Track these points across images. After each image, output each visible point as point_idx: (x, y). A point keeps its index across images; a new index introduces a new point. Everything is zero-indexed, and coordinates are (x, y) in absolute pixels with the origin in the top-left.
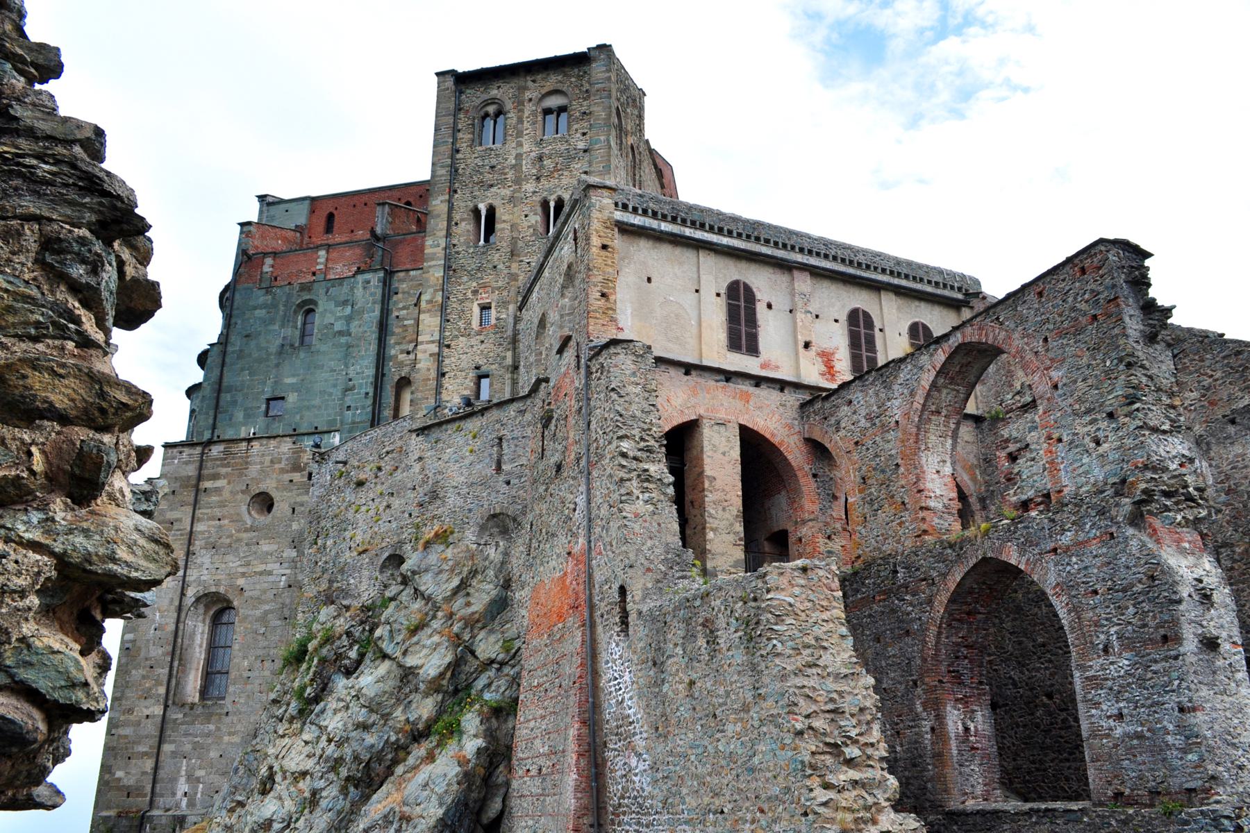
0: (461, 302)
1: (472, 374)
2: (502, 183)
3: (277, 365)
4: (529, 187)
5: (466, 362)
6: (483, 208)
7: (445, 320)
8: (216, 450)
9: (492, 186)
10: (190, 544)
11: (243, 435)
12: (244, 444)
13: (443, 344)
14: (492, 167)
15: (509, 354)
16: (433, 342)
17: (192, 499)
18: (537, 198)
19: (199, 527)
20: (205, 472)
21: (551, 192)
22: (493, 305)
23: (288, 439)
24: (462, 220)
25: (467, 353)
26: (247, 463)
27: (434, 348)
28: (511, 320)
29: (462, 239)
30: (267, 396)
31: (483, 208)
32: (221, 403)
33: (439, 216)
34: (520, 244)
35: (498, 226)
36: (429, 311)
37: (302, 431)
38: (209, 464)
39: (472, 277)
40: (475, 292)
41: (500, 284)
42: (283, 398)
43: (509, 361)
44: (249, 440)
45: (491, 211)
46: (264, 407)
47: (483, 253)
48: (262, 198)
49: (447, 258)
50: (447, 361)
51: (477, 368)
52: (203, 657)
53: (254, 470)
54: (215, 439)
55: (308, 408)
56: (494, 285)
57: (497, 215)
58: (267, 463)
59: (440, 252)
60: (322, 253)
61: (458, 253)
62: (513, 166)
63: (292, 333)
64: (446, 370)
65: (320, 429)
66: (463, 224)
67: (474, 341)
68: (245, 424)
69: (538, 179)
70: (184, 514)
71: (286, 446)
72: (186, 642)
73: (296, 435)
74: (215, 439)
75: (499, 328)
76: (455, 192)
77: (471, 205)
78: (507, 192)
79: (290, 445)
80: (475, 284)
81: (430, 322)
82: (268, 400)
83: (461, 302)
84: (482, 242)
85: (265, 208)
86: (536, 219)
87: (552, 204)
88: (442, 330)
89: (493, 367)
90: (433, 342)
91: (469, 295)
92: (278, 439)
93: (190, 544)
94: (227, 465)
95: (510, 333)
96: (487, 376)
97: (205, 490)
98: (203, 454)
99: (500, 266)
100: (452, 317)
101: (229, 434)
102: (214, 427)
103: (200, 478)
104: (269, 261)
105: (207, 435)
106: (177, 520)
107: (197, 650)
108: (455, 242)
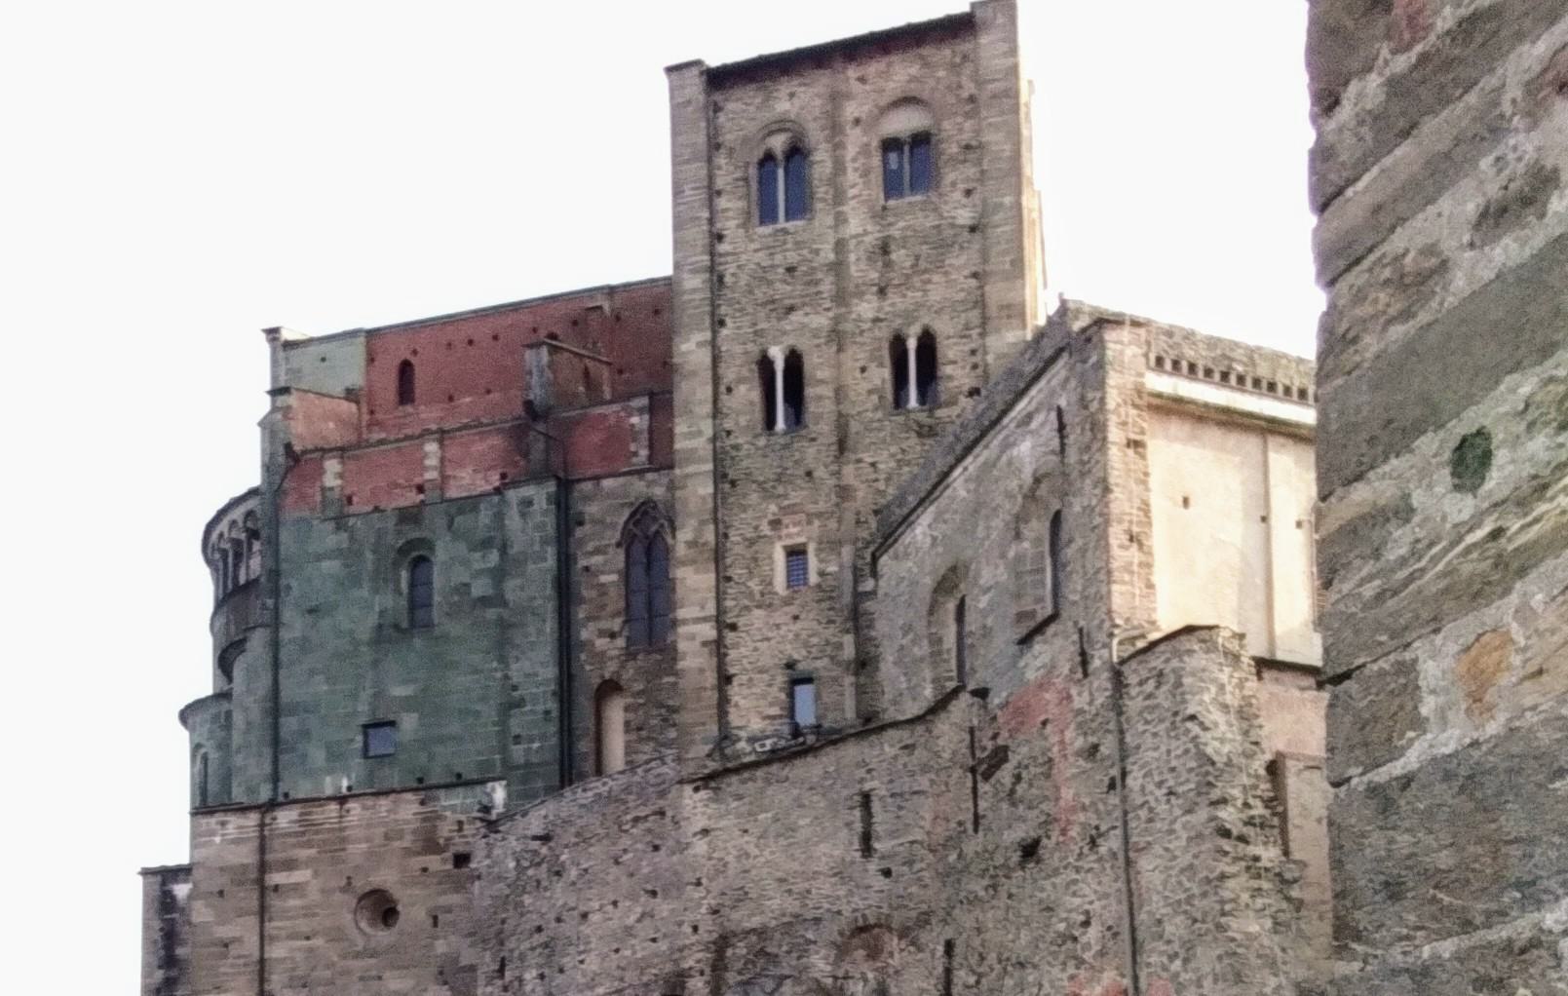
0: (751, 542)
1: (781, 679)
5: (770, 655)
6: (778, 355)
7: (723, 579)
8: (285, 818)
10: (262, 980)
11: (329, 791)
12: (334, 806)
13: (724, 624)
15: (848, 640)
16: (705, 619)
17: (254, 903)
20: (269, 857)
22: (811, 549)
23: (409, 796)
24: (740, 380)
25: (768, 640)
26: (344, 840)
27: (708, 631)
28: (848, 576)
29: (743, 421)
30: (364, 720)
31: (778, 355)
32: (284, 733)
33: (694, 373)
34: (854, 426)
35: (810, 392)
36: (693, 562)
37: (434, 781)
38: (276, 844)
39: (768, 495)
40: (776, 524)
41: (822, 506)
42: (392, 724)
43: (849, 652)
44: (342, 800)
45: (794, 361)
46: (360, 738)
47: (786, 447)
49: (718, 458)
50: (733, 654)
51: (790, 665)
53: (357, 850)
54: (281, 799)
55: (441, 740)
56: (811, 508)
57: (807, 368)
58: (379, 840)
59: (701, 444)
61: (736, 447)
64: (732, 671)
65: (467, 776)
66: (743, 388)
67: (781, 616)
68: (331, 771)
69: (882, 292)
70: (244, 930)
71: (409, 809)
73: (423, 787)
74: (281, 799)
75: (826, 593)
76: (722, 323)
77: (754, 349)
79: (416, 808)
80: (773, 508)
82: (366, 727)
83: (751, 542)
86: (882, 375)
87: (912, 344)
88: (719, 598)
89: (819, 664)
90: (705, 619)
91: (766, 529)
92: (392, 797)
93: (262, 980)
94: (309, 845)
95: (847, 599)
96: (808, 680)
97: (276, 888)
98: (262, 825)
99: (820, 472)
100: (737, 572)
101: (303, 789)
102: (275, 778)
103: (263, 867)
105: (265, 794)
106: (235, 940)
108: (728, 425)
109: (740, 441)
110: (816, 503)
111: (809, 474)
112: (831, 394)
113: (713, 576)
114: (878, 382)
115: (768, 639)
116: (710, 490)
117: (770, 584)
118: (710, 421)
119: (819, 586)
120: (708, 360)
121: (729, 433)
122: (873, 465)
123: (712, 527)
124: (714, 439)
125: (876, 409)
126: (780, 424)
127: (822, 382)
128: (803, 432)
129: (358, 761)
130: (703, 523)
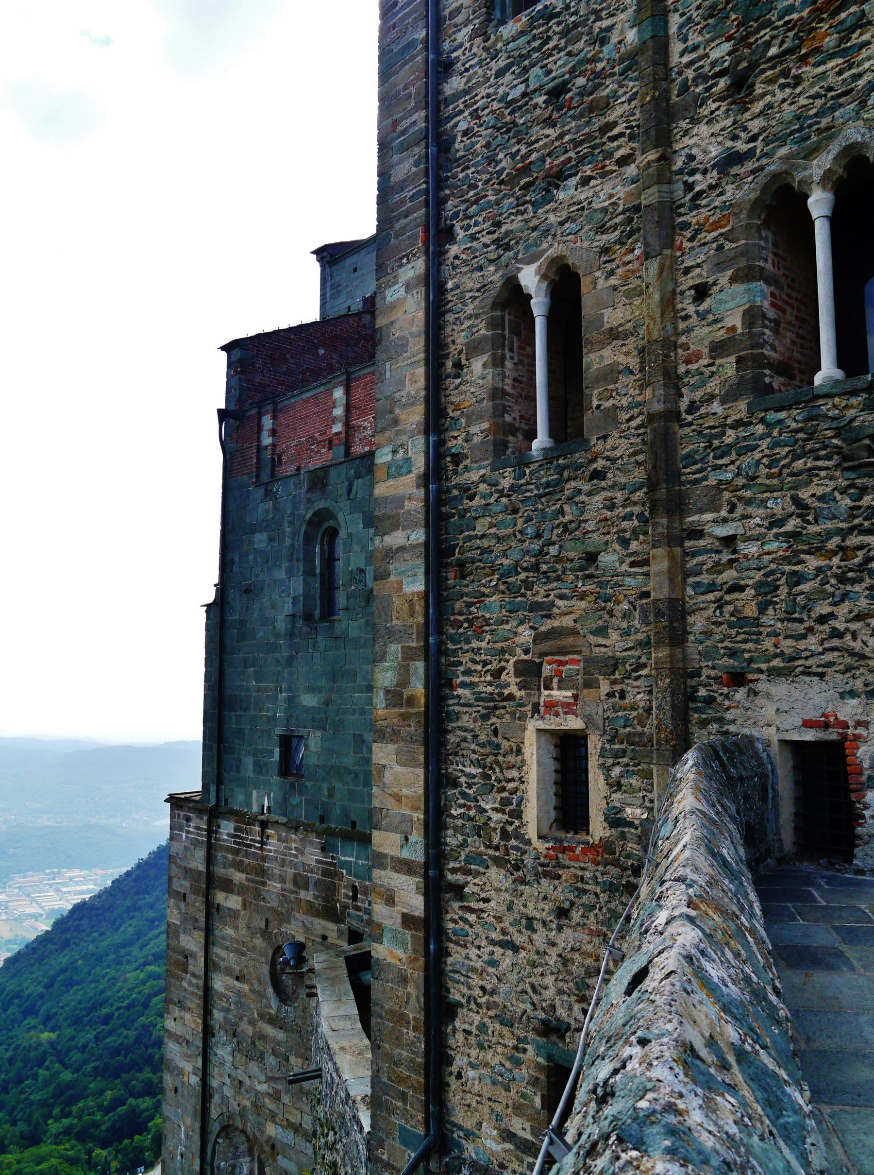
2: (591, 156)
3: (290, 661)
4: (703, 140)
9: (558, 178)
14: (556, 93)
18: (741, 191)
21: (808, 134)
24: (473, 349)
60: (339, 394)
61: (468, 492)
62: (630, 60)
78: (612, 191)
80: (525, 635)
81: (399, 777)
84: (541, 441)
85: (328, 270)
91: (511, 683)
100: (466, 769)
104: (267, 422)
110: (602, 631)
111: (592, 558)
112: (633, 362)
113: (421, 771)
114: (735, 320)
116: (419, 586)
117: (518, 814)
119: (607, 846)
122: (729, 541)
123: (419, 666)
124: (425, 480)
125: (730, 396)
126: (541, 441)
127: (614, 334)
128: (580, 457)
130: (409, 655)
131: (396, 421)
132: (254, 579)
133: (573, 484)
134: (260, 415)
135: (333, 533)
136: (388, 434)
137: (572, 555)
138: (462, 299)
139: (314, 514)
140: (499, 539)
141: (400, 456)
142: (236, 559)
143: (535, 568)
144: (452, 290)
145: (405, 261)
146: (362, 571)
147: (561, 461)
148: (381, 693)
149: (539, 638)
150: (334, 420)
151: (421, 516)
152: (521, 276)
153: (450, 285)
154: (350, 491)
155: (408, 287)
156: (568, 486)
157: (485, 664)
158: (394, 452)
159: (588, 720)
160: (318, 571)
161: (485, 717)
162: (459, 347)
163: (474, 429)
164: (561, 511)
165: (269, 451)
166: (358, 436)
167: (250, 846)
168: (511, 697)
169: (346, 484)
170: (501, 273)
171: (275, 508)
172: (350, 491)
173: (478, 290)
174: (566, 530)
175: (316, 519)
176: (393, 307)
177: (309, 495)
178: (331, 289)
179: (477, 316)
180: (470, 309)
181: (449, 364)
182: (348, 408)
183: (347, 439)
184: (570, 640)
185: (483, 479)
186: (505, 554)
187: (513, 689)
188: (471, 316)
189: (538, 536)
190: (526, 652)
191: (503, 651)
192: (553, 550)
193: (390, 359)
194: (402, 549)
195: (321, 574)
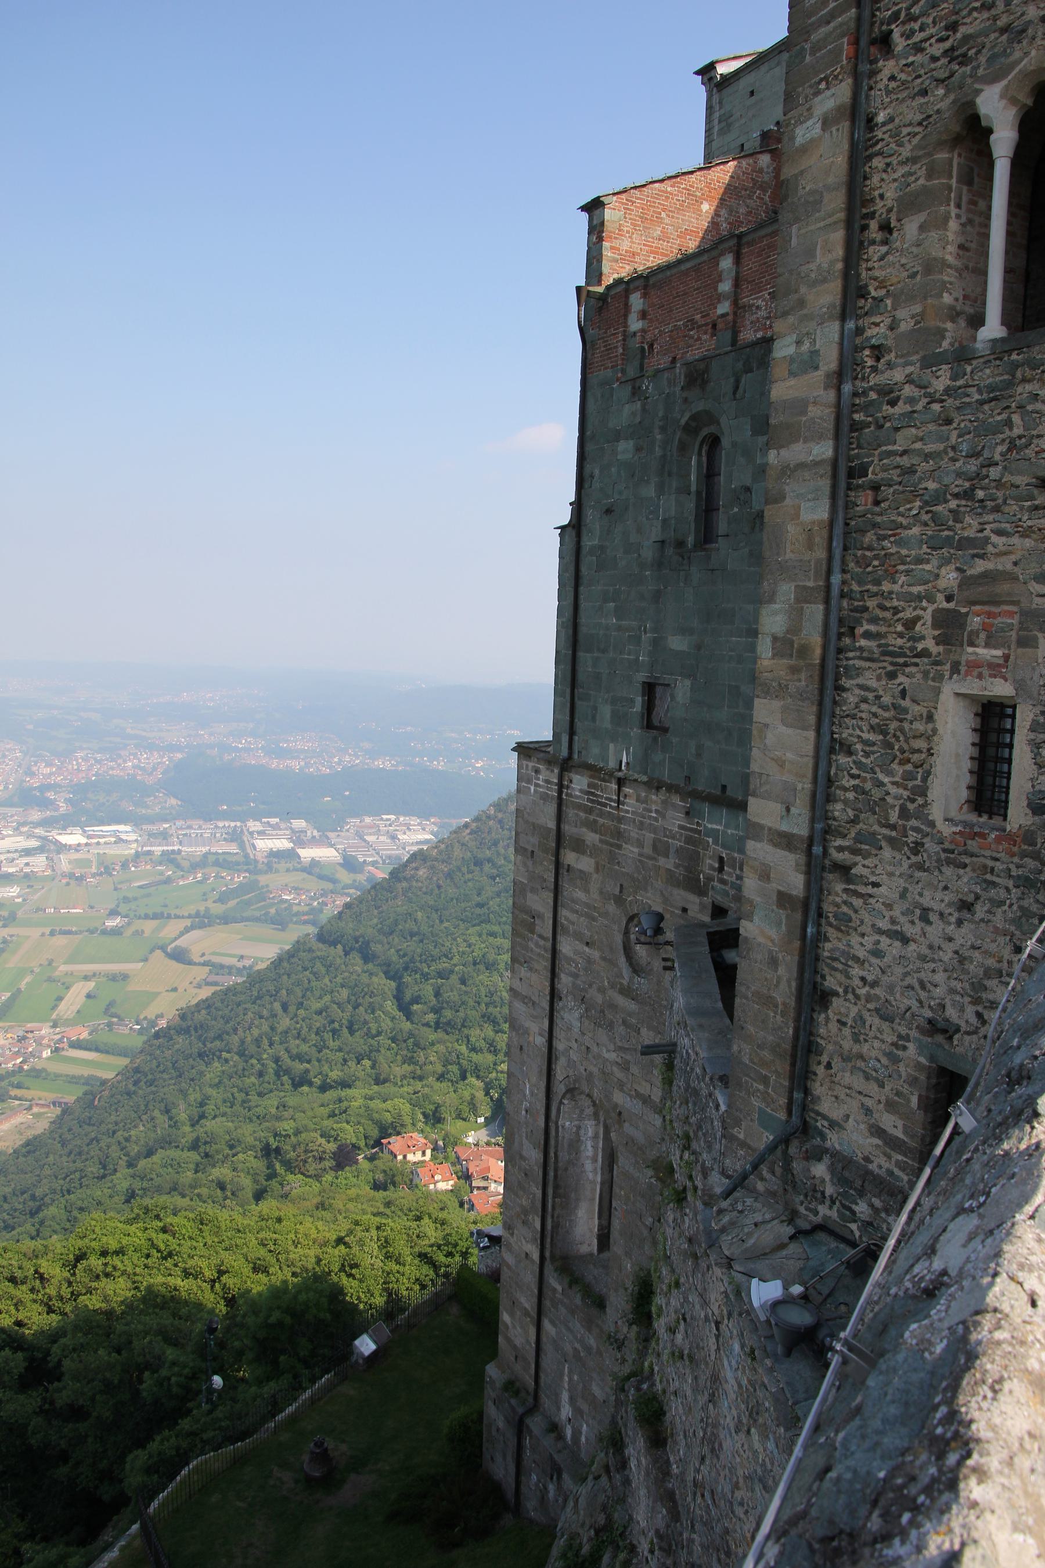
3: (657, 596)
13: (819, 867)
19: (567, 947)
24: (909, 204)
32: (581, 676)
48: (706, 71)
52: (599, 1179)
61: (889, 395)
63: (677, 507)
72: (564, 1156)
76: (885, 42)
80: (949, 578)
81: (781, 742)
84: (993, 328)
104: (636, 301)
107: (589, 1166)
109: (898, 376)
115: (905, 940)
116: (822, 513)
118: (836, 325)
119: (1029, 837)
120: (841, 161)
121: (878, 352)
123: (816, 611)
129: (636, 732)
130: (804, 596)
131: (802, 303)
132: (616, 497)
133: (1028, 387)
134: (627, 293)
135: (714, 442)
136: (791, 319)
137: (1021, 480)
138: (896, 134)
139: (694, 417)
140: (927, 457)
141: (806, 346)
142: (597, 472)
143: (968, 495)
144: (884, 124)
145: (823, 86)
146: (748, 489)
147: (1014, 357)
148: (768, 641)
149: (966, 582)
150: (720, 298)
151: (829, 425)
152: (979, 101)
153: (881, 118)
154: (736, 388)
155: (827, 123)
156: (1020, 389)
157: (896, 611)
158: (798, 343)
159: (1020, 686)
160: (693, 488)
161: (892, 676)
162: (889, 203)
163: (902, 313)
164: (1009, 423)
165: (638, 338)
166: (749, 318)
167: (605, 805)
168: (925, 653)
169: (732, 380)
170: (952, 97)
171: (644, 409)
172: (736, 388)
173: (920, 124)
174: (1012, 446)
175: (694, 424)
176: (804, 149)
177: (684, 395)
178: (720, 122)
179: (914, 160)
180: (906, 152)
181: (874, 225)
182: (737, 284)
183: (735, 322)
184: (1006, 587)
185: (909, 380)
186: (931, 474)
187: (929, 644)
188: (907, 159)
189: (975, 454)
190: (949, 599)
191: (919, 598)
192: (994, 472)
193: (797, 220)
194: (802, 466)
195: (698, 493)
